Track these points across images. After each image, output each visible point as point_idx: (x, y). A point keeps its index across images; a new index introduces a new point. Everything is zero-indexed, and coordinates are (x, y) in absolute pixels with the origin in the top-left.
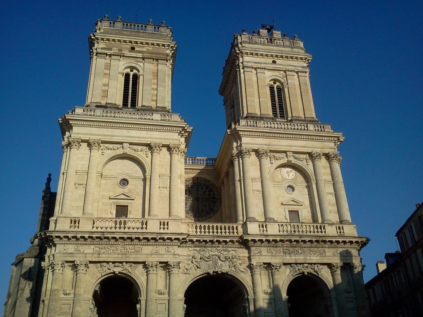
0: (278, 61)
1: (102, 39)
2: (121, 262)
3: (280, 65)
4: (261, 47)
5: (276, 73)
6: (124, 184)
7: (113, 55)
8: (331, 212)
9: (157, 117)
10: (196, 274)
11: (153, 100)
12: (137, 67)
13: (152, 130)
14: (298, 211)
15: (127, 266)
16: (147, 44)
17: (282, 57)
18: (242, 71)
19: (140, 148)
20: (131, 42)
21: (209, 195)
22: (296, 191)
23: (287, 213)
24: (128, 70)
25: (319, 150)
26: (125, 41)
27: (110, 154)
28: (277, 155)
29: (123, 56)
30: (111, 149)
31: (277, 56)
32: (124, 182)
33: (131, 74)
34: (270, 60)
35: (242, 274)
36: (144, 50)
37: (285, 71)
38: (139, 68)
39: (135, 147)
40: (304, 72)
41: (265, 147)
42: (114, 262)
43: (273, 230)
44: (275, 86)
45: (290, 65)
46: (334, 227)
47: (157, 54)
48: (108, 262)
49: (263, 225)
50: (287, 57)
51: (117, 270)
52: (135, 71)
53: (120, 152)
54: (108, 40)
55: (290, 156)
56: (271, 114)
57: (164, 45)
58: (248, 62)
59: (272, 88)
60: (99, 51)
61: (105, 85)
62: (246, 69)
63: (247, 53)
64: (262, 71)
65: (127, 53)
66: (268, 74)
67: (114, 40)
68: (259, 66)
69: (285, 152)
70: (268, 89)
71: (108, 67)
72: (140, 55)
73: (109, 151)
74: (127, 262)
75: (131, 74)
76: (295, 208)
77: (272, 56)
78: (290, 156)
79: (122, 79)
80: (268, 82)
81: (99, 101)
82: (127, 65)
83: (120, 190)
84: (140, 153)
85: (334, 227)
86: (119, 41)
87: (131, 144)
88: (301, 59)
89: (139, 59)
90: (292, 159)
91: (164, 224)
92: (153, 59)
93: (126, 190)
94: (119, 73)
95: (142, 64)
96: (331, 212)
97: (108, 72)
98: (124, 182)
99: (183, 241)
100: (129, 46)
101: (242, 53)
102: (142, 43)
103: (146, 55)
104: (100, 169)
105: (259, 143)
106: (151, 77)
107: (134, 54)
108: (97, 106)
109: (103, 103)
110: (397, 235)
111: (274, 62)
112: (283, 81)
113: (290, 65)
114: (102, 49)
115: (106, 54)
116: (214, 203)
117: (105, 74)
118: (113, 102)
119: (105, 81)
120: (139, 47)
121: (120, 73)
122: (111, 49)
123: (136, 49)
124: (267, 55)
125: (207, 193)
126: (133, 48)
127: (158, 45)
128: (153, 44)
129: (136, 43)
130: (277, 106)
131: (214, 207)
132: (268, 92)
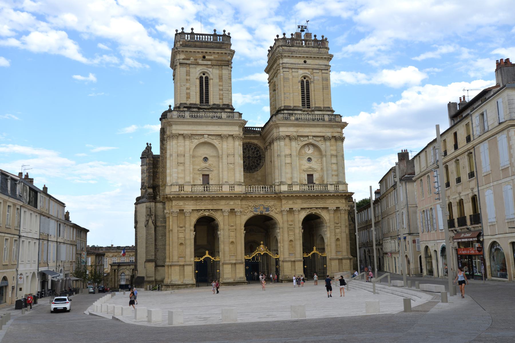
0: (308, 61)
1: (183, 51)
2: (209, 210)
3: (309, 64)
4: (296, 48)
5: (306, 71)
6: (206, 160)
7: (191, 64)
8: (333, 175)
9: (224, 115)
10: (251, 215)
11: (220, 99)
12: (208, 72)
13: (221, 125)
14: (312, 175)
15: (212, 212)
16: (214, 53)
17: (311, 57)
18: (282, 70)
19: (214, 137)
20: (202, 52)
21: (257, 154)
22: (313, 162)
23: (306, 176)
24: (202, 75)
25: (329, 135)
26: (198, 52)
27: (196, 142)
28: (302, 139)
29: (198, 64)
30: (197, 139)
31: (307, 57)
32: (206, 159)
33: (204, 76)
34: (302, 61)
35: (277, 215)
36: (212, 57)
37: (313, 69)
38: (210, 73)
39: (212, 138)
40: (326, 70)
41: (295, 134)
42: (205, 210)
43: (296, 188)
44: (305, 80)
45: (316, 65)
46: (333, 186)
47: (221, 61)
48: (202, 210)
49: (290, 185)
50: (314, 57)
51: (207, 214)
52: (206, 75)
53: (202, 140)
54: (187, 51)
55: (311, 139)
56: (301, 105)
57: (226, 53)
58: (286, 63)
59: (302, 82)
60: (181, 61)
61: (187, 89)
62: (285, 70)
63: (285, 56)
64: (296, 70)
65: (201, 62)
66: (301, 72)
67: (191, 52)
68: (294, 66)
69: (308, 136)
70: (300, 84)
71: (188, 74)
72: (209, 63)
73: (196, 141)
74: (212, 210)
75: (204, 76)
76: (311, 173)
77: (303, 57)
78: (311, 139)
79: (198, 82)
80: (300, 79)
81: (185, 102)
82: (201, 71)
83: (204, 165)
84: (215, 141)
85: (333, 186)
86: (195, 52)
87: (209, 135)
88: (325, 58)
89: (209, 66)
90: (311, 141)
91: (232, 187)
92: (219, 65)
93: (206, 165)
94: (196, 79)
95: (210, 70)
96: (333, 175)
97: (188, 78)
98: (206, 159)
99: (243, 197)
100: (201, 56)
101: (282, 56)
102: (210, 53)
103: (214, 62)
104: (191, 153)
105: (291, 131)
106: (218, 80)
107: (205, 62)
108: (185, 107)
109: (188, 102)
110: (380, 182)
111: (305, 62)
112: (310, 77)
113: (316, 65)
114: (183, 59)
115: (186, 64)
116: (260, 160)
117: (187, 79)
118: (194, 102)
119: (188, 85)
120: (208, 55)
121: (196, 79)
122: (189, 59)
123: (207, 57)
124: (300, 57)
125: (255, 153)
126: (204, 57)
127: (222, 53)
128: (218, 53)
129: (206, 53)
130: (305, 96)
131: (260, 162)
132: (300, 88)
